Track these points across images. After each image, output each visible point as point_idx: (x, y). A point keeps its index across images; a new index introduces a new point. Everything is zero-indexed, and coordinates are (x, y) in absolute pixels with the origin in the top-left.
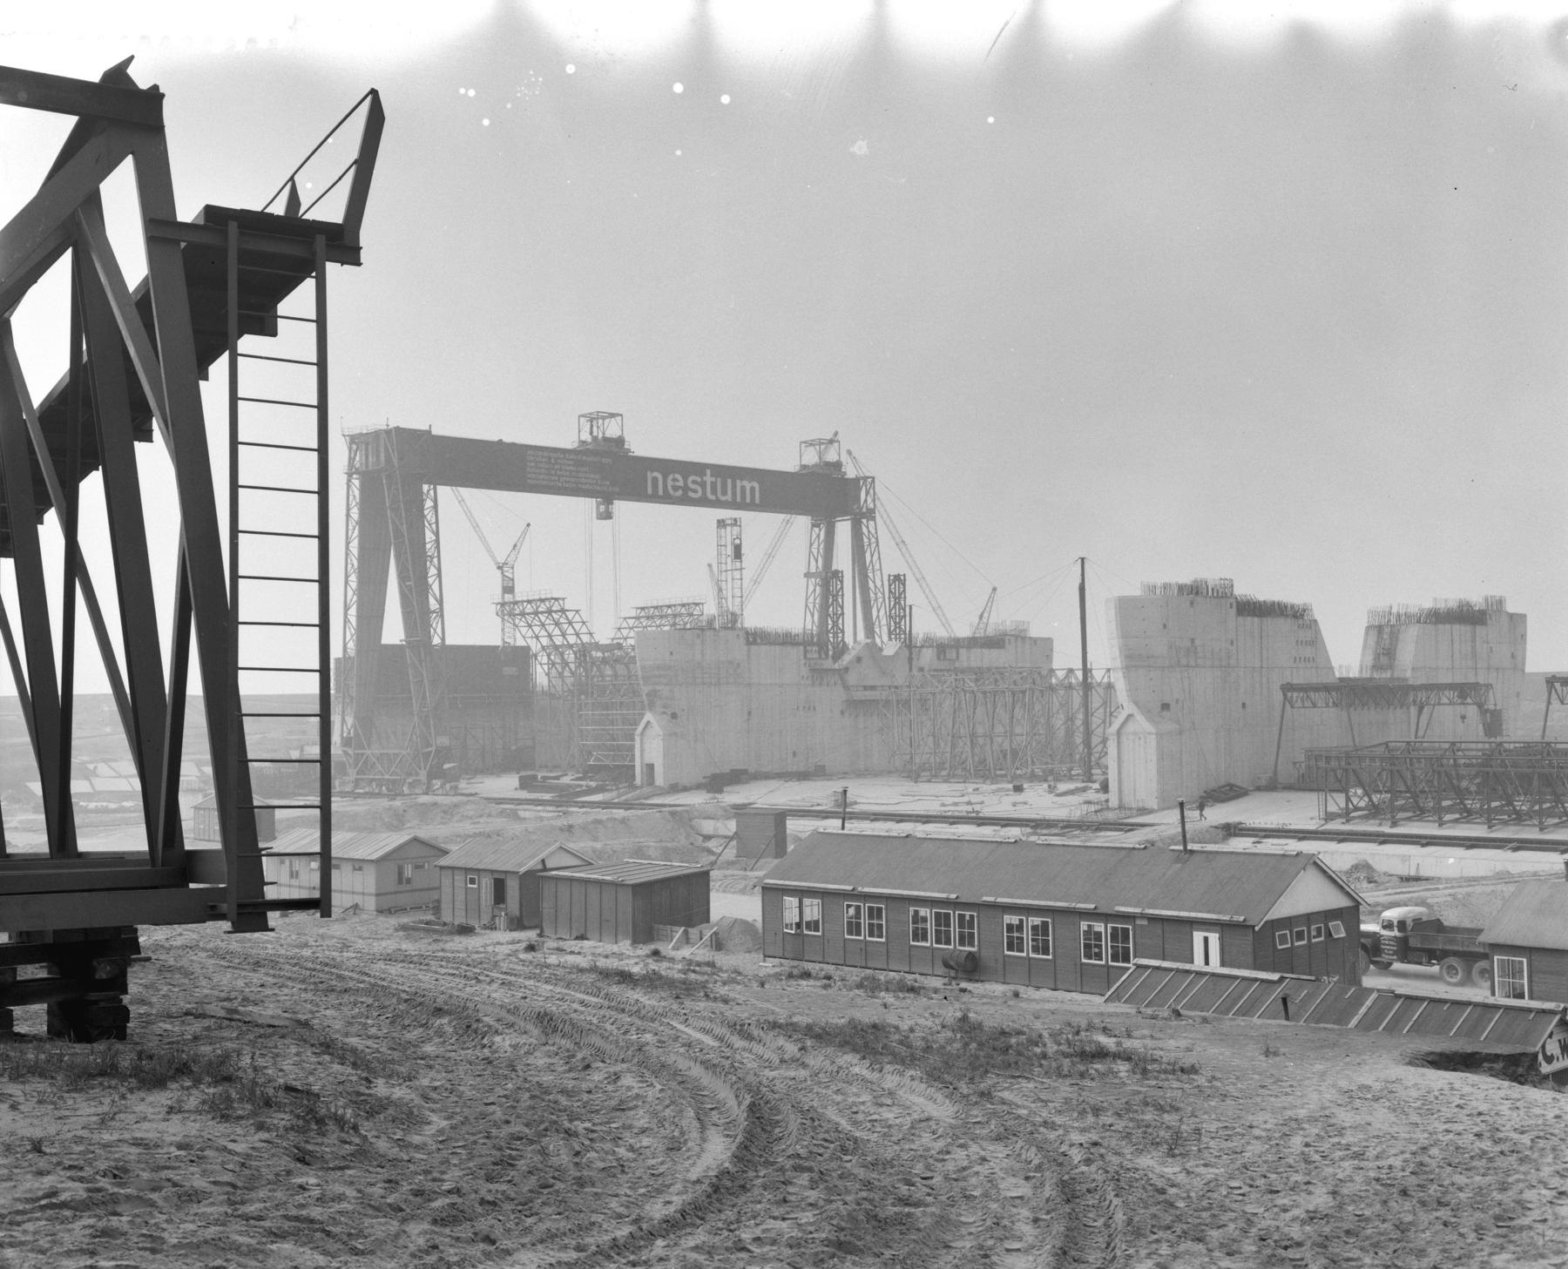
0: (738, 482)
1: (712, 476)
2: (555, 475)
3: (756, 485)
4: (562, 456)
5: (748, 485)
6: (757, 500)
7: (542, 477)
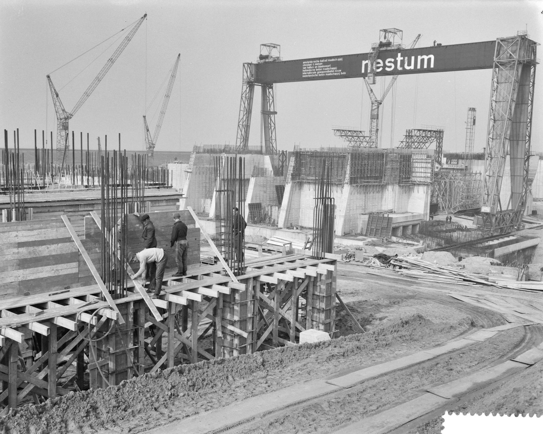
0: (420, 58)
1: (401, 56)
2: (315, 71)
3: (432, 57)
4: (319, 61)
5: (426, 58)
6: (432, 66)
7: (309, 73)
